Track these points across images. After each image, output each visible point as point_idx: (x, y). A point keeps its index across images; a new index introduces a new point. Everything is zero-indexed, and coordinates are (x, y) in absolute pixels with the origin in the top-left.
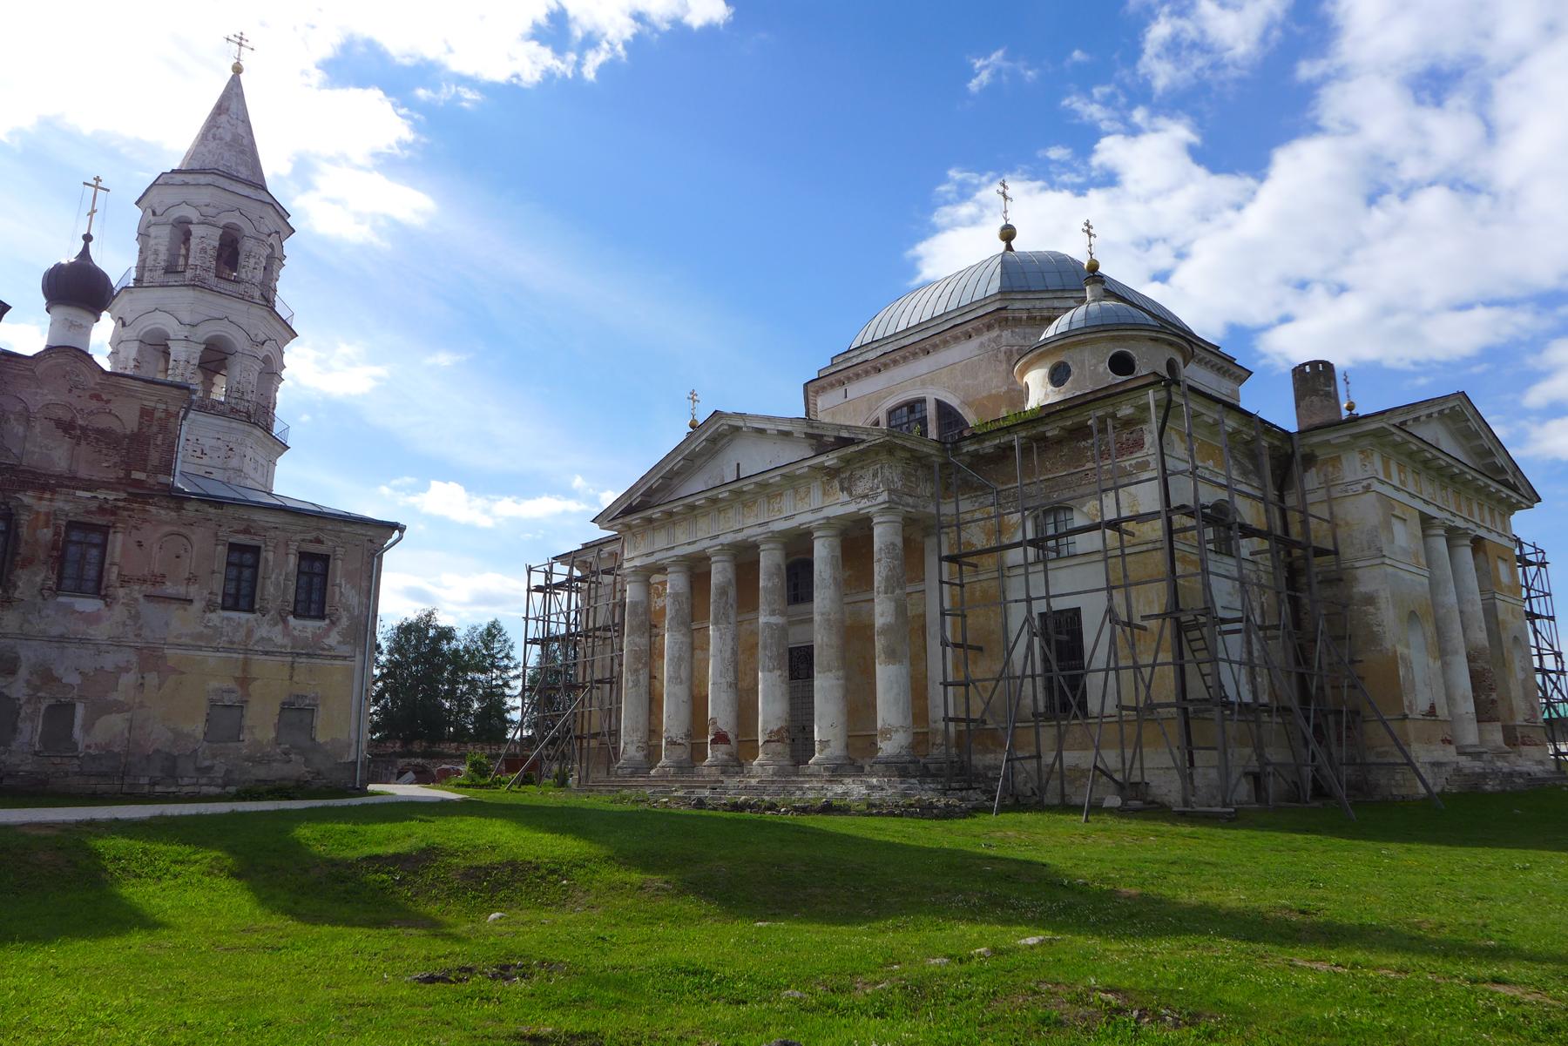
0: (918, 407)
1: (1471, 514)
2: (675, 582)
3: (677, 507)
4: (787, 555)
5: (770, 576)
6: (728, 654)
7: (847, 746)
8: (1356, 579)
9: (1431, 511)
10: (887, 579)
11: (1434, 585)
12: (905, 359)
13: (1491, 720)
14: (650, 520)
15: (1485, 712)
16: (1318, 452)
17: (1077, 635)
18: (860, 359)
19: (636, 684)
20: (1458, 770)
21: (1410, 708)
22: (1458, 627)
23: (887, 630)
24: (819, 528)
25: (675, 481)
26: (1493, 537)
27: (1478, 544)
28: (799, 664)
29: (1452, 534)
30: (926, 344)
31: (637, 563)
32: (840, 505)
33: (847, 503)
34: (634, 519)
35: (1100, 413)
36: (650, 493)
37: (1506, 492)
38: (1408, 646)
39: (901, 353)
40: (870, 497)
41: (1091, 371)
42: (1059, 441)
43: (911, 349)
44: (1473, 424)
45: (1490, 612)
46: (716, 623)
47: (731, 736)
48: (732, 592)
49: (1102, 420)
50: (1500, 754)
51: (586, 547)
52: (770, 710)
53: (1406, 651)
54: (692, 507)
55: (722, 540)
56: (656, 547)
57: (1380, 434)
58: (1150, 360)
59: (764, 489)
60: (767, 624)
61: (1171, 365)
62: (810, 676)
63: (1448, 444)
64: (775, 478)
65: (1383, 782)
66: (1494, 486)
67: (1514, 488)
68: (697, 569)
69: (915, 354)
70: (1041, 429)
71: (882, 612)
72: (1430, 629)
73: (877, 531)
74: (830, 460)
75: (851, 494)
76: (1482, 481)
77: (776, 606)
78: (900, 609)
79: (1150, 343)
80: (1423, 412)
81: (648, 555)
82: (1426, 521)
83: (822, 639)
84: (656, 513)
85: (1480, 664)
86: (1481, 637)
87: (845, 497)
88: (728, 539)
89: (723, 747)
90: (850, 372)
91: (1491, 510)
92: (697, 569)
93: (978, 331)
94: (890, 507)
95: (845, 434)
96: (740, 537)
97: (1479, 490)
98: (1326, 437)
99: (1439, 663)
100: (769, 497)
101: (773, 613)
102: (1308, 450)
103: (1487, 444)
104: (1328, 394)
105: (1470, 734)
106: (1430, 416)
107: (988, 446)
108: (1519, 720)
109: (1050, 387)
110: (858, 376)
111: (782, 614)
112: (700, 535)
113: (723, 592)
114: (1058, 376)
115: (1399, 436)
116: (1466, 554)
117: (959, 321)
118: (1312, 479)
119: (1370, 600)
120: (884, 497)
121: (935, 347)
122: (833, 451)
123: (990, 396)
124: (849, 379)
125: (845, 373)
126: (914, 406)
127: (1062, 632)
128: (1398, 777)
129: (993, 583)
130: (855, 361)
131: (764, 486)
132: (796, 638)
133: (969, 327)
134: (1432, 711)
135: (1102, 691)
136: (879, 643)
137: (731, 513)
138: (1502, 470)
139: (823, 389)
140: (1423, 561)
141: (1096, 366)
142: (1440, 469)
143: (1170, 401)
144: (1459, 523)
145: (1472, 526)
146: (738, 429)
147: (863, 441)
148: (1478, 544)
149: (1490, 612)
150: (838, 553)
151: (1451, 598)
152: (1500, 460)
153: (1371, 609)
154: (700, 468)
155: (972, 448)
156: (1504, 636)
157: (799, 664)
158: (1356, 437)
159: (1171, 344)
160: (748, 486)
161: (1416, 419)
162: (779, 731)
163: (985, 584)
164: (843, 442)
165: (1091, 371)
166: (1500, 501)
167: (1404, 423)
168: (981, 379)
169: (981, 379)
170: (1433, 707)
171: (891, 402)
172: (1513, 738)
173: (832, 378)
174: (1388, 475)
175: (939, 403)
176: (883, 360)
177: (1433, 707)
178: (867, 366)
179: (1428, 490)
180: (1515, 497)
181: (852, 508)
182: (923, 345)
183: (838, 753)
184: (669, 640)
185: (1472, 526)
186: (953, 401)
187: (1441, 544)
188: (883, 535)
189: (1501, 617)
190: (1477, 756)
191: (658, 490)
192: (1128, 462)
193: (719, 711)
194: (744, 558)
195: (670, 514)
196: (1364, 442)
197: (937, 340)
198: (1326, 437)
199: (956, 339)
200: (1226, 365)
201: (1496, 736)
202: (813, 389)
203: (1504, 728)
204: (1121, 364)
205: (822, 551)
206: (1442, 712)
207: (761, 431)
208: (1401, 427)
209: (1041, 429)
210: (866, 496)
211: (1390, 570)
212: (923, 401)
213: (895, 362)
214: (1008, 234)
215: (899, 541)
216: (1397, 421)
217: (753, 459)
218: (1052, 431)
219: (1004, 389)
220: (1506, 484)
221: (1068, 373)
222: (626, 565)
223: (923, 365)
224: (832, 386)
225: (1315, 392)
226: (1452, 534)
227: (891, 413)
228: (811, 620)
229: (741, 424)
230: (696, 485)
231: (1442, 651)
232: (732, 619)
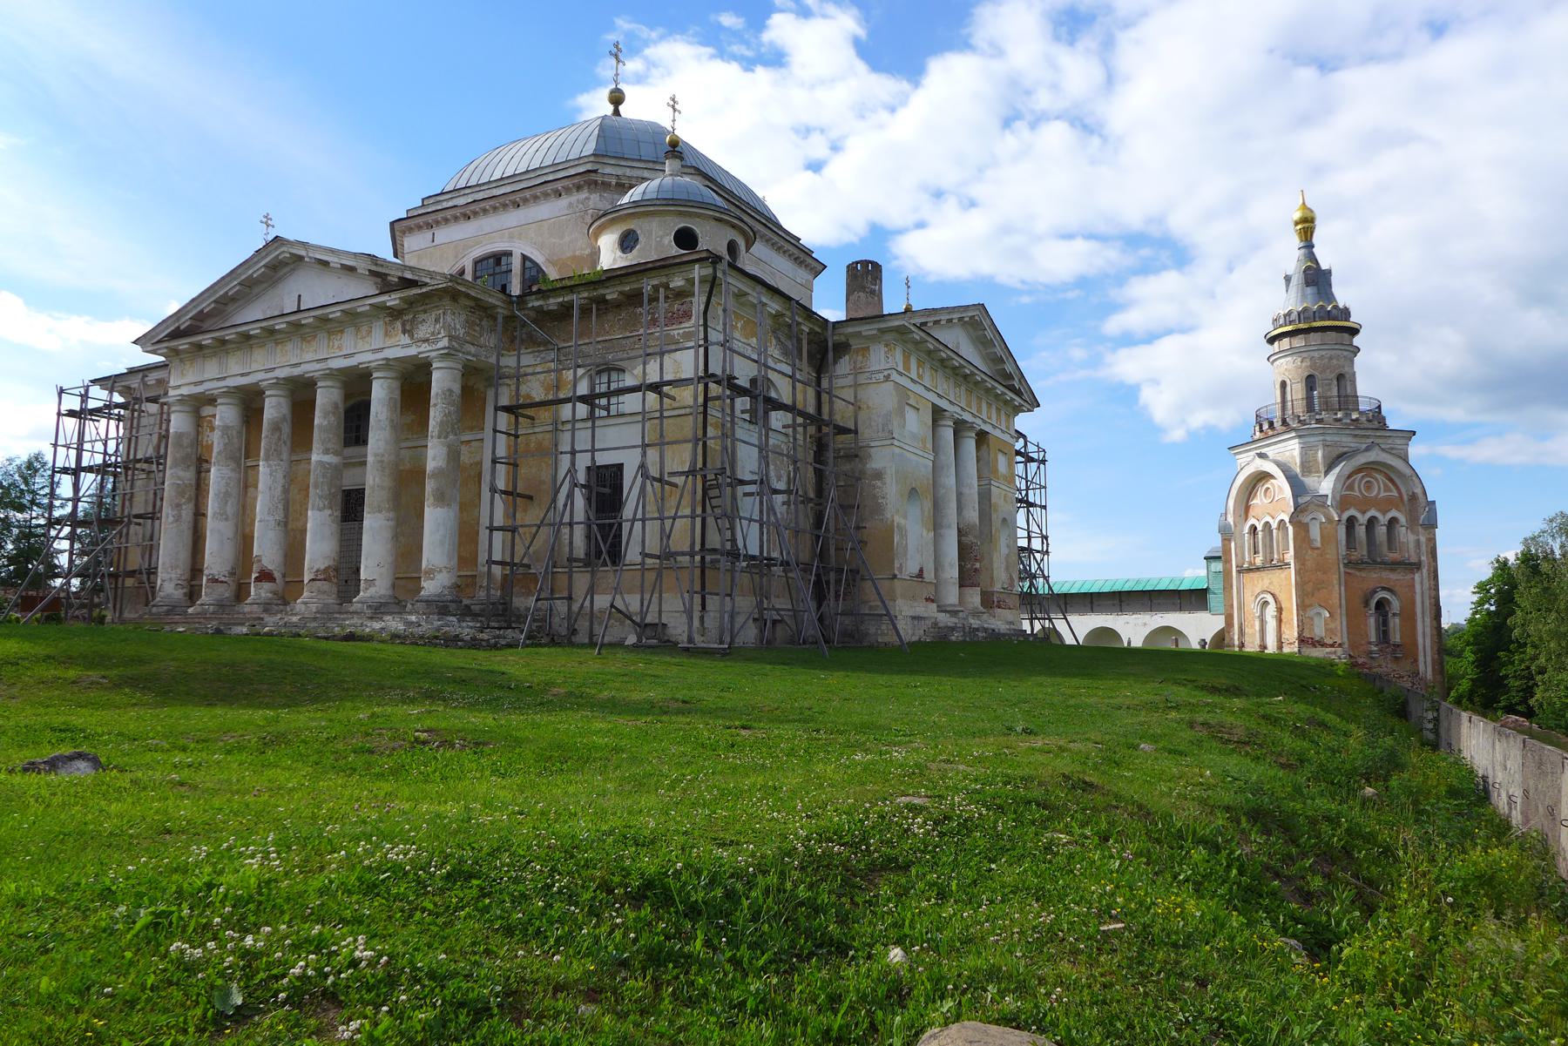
0: (504, 260)
1: (979, 410)
2: (225, 415)
3: (230, 335)
4: (347, 397)
5: (325, 417)
6: (278, 491)
7: (394, 586)
9: (943, 404)
10: (442, 424)
11: (936, 468)
12: (495, 208)
13: (973, 585)
14: (199, 347)
15: (966, 579)
16: (852, 342)
17: (618, 488)
18: (450, 204)
19: (178, 519)
20: (935, 624)
21: (900, 569)
22: (954, 505)
23: (434, 475)
24: (378, 369)
25: (230, 308)
26: (997, 433)
27: (982, 437)
28: (351, 506)
29: (960, 427)
30: (517, 197)
31: (185, 391)
32: (400, 347)
33: (408, 346)
34: (182, 344)
35: (655, 282)
36: (201, 317)
37: (1010, 395)
38: (905, 517)
39: (492, 202)
40: (430, 339)
41: (658, 241)
42: (618, 305)
43: (501, 200)
44: (989, 334)
45: (985, 497)
46: (267, 459)
47: (277, 575)
48: (286, 429)
49: (656, 288)
50: (976, 614)
51: (132, 372)
52: (319, 548)
53: (903, 522)
54: (247, 337)
56: (207, 376)
57: (902, 331)
58: (712, 238)
59: (325, 323)
60: (320, 463)
61: (732, 248)
62: (359, 519)
63: (969, 351)
64: (335, 313)
65: (872, 630)
66: (1000, 389)
67: (1018, 393)
68: (250, 401)
69: (505, 206)
70: (602, 291)
71: (435, 456)
72: (928, 505)
73: (435, 376)
74: (392, 300)
75: (412, 337)
76: (990, 383)
77: (330, 446)
78: (453, 455)
79: (714, 223)
80: (944, 317)
81: (196, 384)
82: (937, 413)
83: (374, 481)
84: (206, 339)
85: (970, 539)
86: (972, 515)
87: (406, 339)
88: (282, 373)
89: (267, 586)
90: (439, 216)
91: (998, 410)
92: (250, 401)
93: (568, 190)
94: (448, 355)
95: (408, 275)
96: (296, 371)
97: (988, 391)
98: (857, 329)
99: (932, 534)
100: (330, 333)
101: (326, 452)
102: (843, 339)
103: (999, 351)
104: (873, 292)
105: (951, 596)
106: (950, 321)
107: (553, 303)
108: (997, 587)
109: (619, 253)
110: (446, 220)
111: (336, 453)
112: (255, 367)
113: (276, 428)
114: (627, 242)
115: (918, 335)
116: (970, 445)
117: (551, 177)
118: (844, 366)
119: (879, 475)
120: (445, 342)
121: (525, 200)
122: (400, 292)
123: (574, 258)
124: (438, 223)
125: (433, 216)
126: (498, 258)
127: (606, 487)
129: (548, 436)
130: (445, 205)
131: (324, 320)
132: (349, 482)
133: (559, 185)
134: (920, 574)
135: (639, 540)
136: (430, 486)
137: (289, 346)
138: (1010, 377)
139: (410, 230)
140: (929, 446)
142: (954, 368)
143: (715, 277)
144: (967, 417)
145: (978, 421)
146: (301, 258)
147: (426, 284)
148: (982, 437)
149: (985, 497)
150: (397, 395)
151: (950, 480)
152: (1009, 368)
153: (879, 483)
154: (258, 296)
155: (537, 304)
156: (994, 516)
157: (351, 506)
158: (883, 331)
159: (734, 226)
160: (307, 319)
161: (936, 322)
162: (326, 570)
163: (540, 437)
164: (408, 284)
165: (658, 241)
166: (1006, 402)
167: (925, 324)
168: (567, 239)
169: (567, 239)
170: (921, 570)
171: (478, 252)
172: (989, 601)
173: (420, 220)
174: (907, 367)
175: (525, 258)
176: (472, 207)
177: (921, 570)
178: (457, 212)
179: (943, 386)
180: (1018, 401)
181: (412, 351)
182: (512, 197)
183: (383, 592)
184: (217, 476)
185: (978, 421)
186: (539, 258)
187: (948, 434)
188: (442, 381)
189: (993, 501)
190: (954, 613)
191: (210, 315)
192: (677, 331)
193: (267, 549)
194: (301, 393)
195: (223, 342)
196: (889, 337)
197: (527, 194)
198: (857, 329)
199: (546, 195)
200: (802, 256)
201: (974, 598)
202: (399, 229)
203: (983, 594)
204: (685, 239)
205: (381, 393)
206: (929, 575)
207: (325, 264)
208: (922, 327)
209: (602, 291)
210: (426, 340)
211: (897, 450)
212: (509, 254)
213: (485, 211)
214: (617, 99)
215: (457, 388)
216: (918, 321)
217: (315, 292)
218: (611, 294)
219: (588, 251)
220: (1012, 389)
222: (171, 393)
223: (512, 218)
224: (420, 227)
225: (863, 289)
226: (960, 427)
227: (477, 262)
228: (364, 463)
229: (303, 253)
231: (937, 525)
232: (285, 456)
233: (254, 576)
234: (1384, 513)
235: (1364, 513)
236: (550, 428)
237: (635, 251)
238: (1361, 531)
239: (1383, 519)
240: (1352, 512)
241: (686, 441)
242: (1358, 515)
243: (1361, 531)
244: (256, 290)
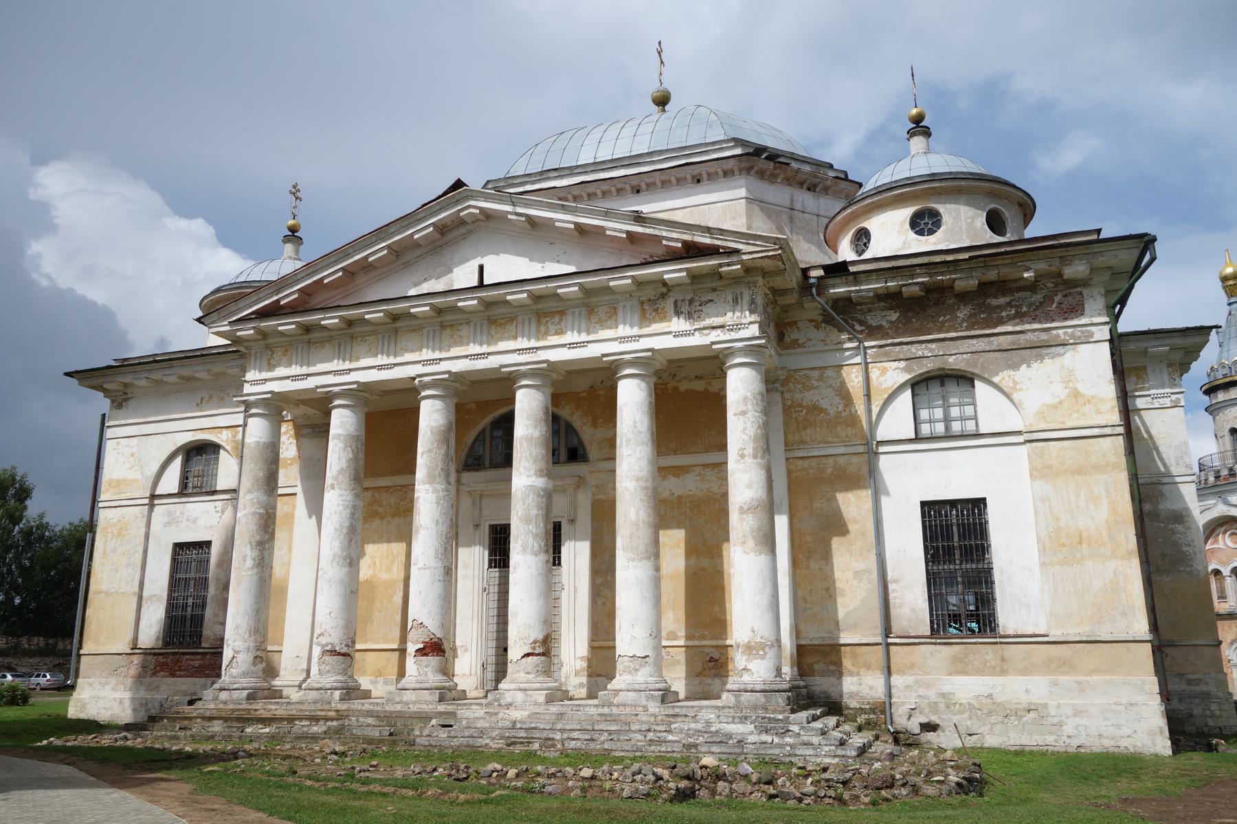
3: (374, 314)
8: (1162, 495)
24: (633, 363)
39: (605, 187)
42: (963, 297)
74: (673, 272)
96: (480, 364)
109: (912, 235)
121: (650, 186)
128: (1214, 707)
129: (855, 459)
130: (529, 188)
133: (703, 170)
141: (973, 218)
146: (502, 216)
153: (1180, 528)
154: (407, 265)
163: (841, 460)
222: (247, 389)
236: (861, 449)
237: (939, 234)
241: (1097, 468)
244: (406, 258)
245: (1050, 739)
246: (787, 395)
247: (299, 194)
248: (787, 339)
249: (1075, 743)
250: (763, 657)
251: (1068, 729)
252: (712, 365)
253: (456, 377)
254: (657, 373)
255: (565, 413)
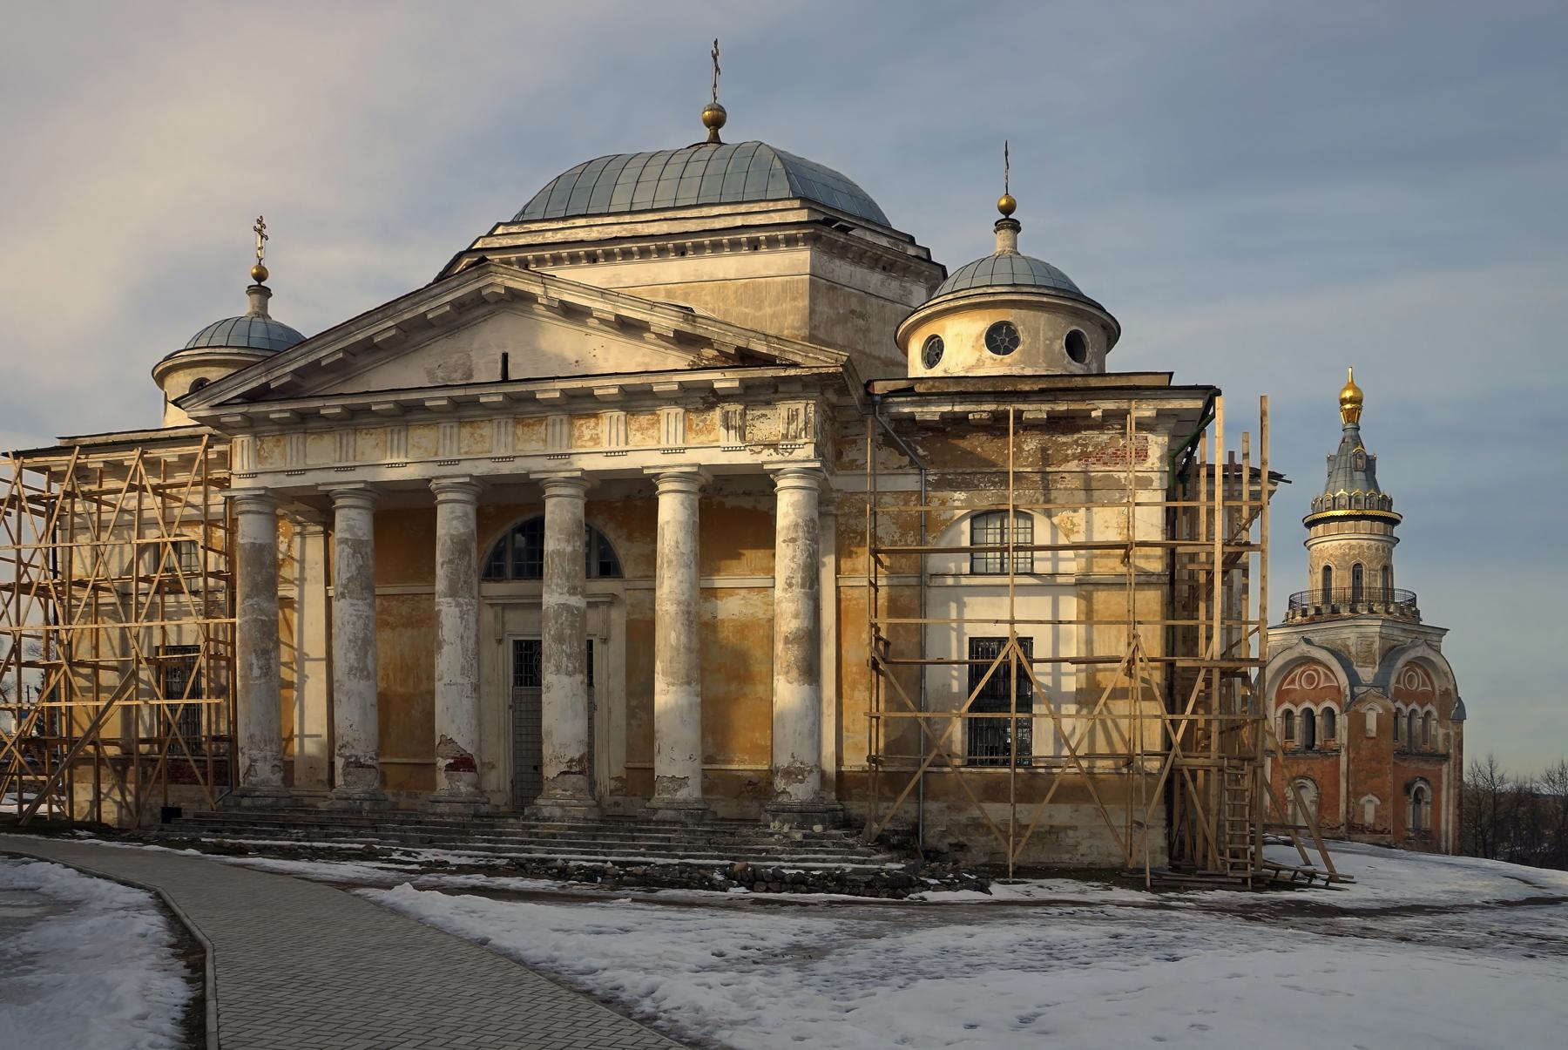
18: (559, 237)
33: (735, 449)
46: (453, 592)
55: (465, 468)
56: (311, 462)
69: (662, 252)
75: (743, 438)
81: (290, 473)
87: (733, 439)
88: (483, 468)
93: (772, 243)
107: (933, 412)
113: (461, 547)
114: (1000, 339)
129: (907, 592)
168: (768, 311)
181: (745, 458)
199: (735, 246)
210: (774, 446)
221: (1015, 342)
230: (231, 371)
233: (442, 763)
234: (1317, 704)
235: (1317, 704)
236: (913, 581)
238: (1404, 723)
239: (1421, 713)
240: (1287, 706)
242: (1403, 707)
243: (1404, 723)
245: (1066, 857)
246: (841, 520)
247: (265, 232)
248: (845, 459)
249: (1087, 860)
250: (801, 782)
251: (1082, 849)
252: (760, 484)
253: (482, 480)
254: (702, 489)
255: (599, 522)
